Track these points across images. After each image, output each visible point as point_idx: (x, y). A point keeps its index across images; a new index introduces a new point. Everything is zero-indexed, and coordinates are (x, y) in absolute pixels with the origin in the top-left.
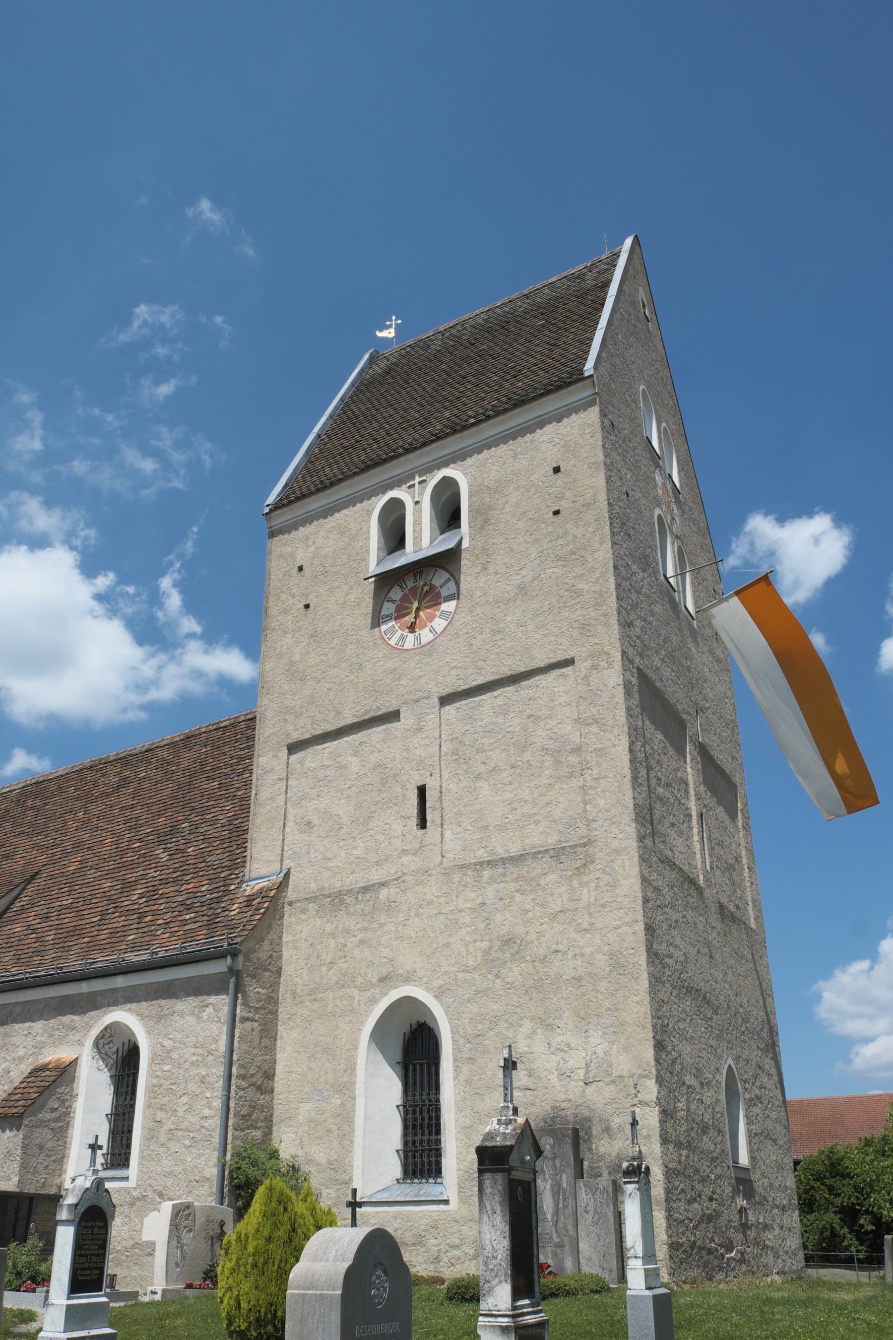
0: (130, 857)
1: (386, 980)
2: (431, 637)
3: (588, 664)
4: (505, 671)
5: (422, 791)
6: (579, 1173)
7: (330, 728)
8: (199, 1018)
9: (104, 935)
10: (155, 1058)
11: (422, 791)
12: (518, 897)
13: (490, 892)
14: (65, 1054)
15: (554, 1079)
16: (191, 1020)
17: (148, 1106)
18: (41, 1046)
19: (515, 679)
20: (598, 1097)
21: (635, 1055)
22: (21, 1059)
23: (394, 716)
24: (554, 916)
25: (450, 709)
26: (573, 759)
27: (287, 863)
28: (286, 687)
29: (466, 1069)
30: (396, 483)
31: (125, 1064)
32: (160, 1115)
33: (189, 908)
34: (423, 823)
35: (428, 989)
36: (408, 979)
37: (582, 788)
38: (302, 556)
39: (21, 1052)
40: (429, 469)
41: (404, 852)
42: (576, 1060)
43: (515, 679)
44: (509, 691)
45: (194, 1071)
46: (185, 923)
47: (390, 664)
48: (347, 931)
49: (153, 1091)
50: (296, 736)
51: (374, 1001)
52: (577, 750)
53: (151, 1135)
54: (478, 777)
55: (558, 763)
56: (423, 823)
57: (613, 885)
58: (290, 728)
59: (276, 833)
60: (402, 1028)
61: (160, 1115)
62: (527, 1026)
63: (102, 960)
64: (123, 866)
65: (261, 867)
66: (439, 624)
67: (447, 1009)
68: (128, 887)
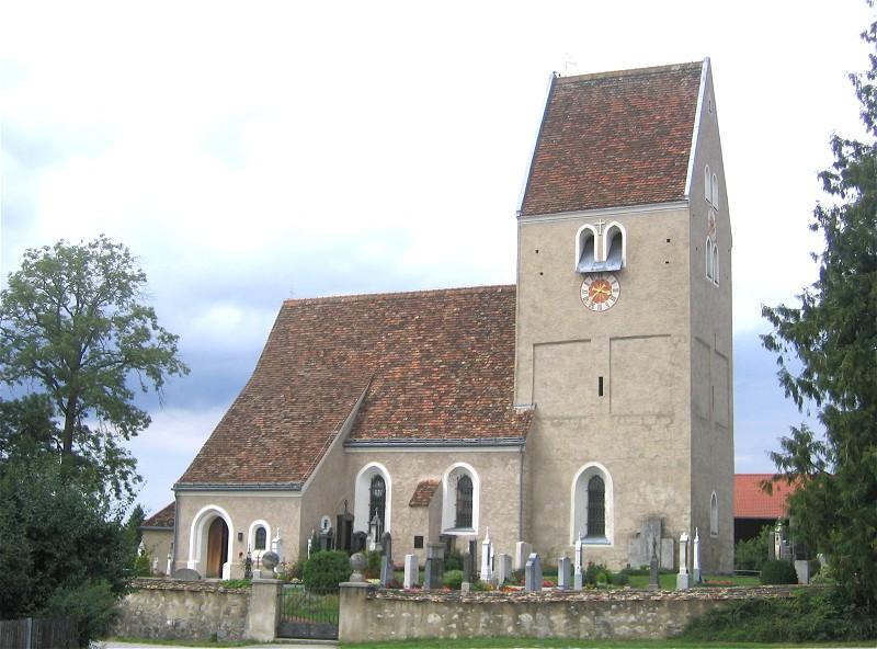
1: (588, 460)
3: (676, 339)
5: (601, 379)
6: (662, 537)
8: (504, 470)
11: (601, 379)
14: (434, 478)
15: (653, 503)
18: (417, 475)
20: (670, 510)
21: (684, 499)
22: (407, 478)
23: (590, 340)
24: (656, 442)
26: (668, 378)
27: (536, 401)
28: (532, 314)
29: (618, 497)
31: (464, 486)
34: (601, 394)
35: (603, 464)
36: (594, 460)
37: (671, 391)
39: (407, 475)
41: (592, 405)
42: (663, 496)
46: (487, 424)
48: (566, 436)
50: (538, 341)
51: (579, 467)
52: (670, 375)
53: (483, 514)
54: (627, 378)
55: (661, 378)
56: (601, 394)
57: (681, 433)
59: (530, 387)
60: (589, 477)
62: (644, 483)
64: (432, 382)
65: (522, 404)
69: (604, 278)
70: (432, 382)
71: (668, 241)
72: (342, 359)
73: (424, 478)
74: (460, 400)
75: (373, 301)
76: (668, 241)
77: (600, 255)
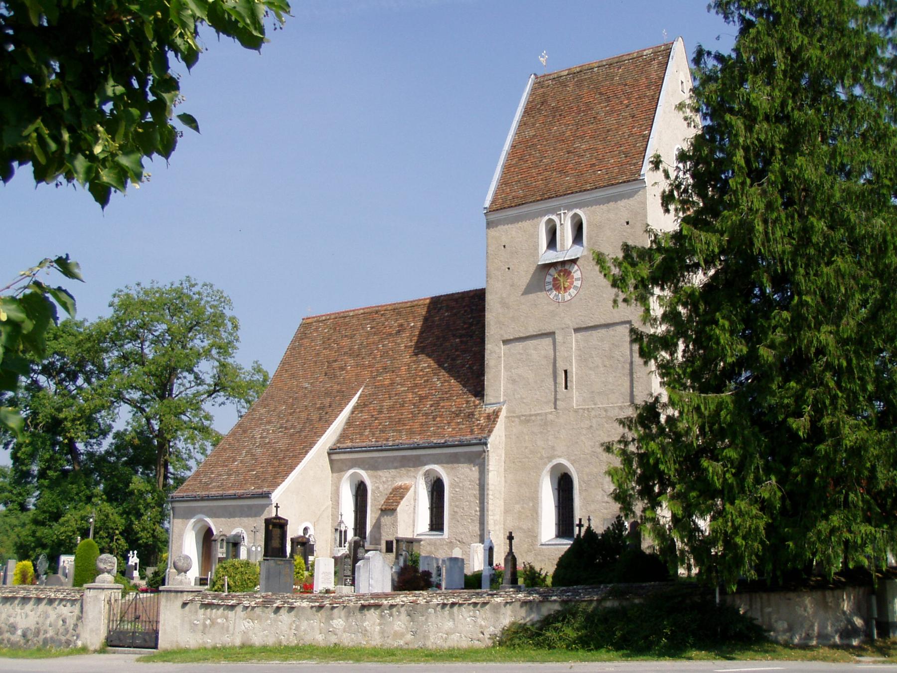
0: (419, 381)
2: (569, 298)
4: (603, 322)
7: (522, 335)
9: (417, 425)
10: (452, 486)
12: (606, 425)
13: (594, 421)
16: (468, 470)
17: (450, 505)
18: (394, 478)
19: (607, 326)
25: (579, 335)
29: (584, 494)
30: (554, 211)
32: (456, 509)
33: (457, 415)
36: (560, 457)
38: (504, 240)
40: (569, 207)
43: (607, 326)
44: (603, 331)
45: (470, 492)
46: (459, 424)
47: (551, 308)
49: (452, 499)
51: (546, 464)
58: (502, 332)
61: (456, 509)
63: (417, 439)
64: (416, 385)
66: (573, 291)
67: (576, 469)
68: (422, 398)
69: (567, 267)
70: (416, 385)
71: (628, 223)
72: (342, 369)
73: (399, 483)
74: (436, 404)
75: (377, 312)
76: (628, 223)
77: (562, 245)
